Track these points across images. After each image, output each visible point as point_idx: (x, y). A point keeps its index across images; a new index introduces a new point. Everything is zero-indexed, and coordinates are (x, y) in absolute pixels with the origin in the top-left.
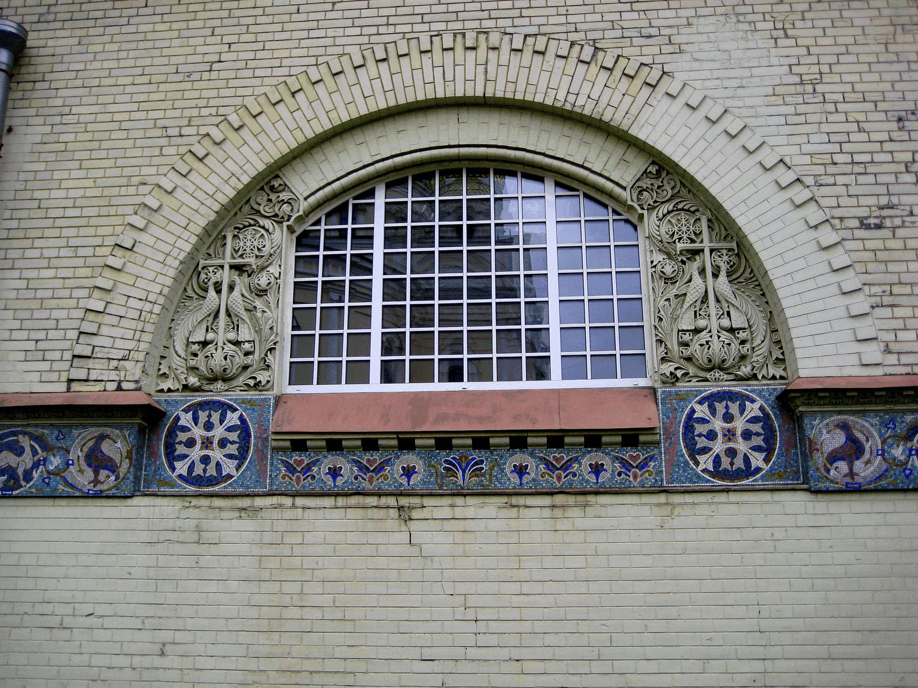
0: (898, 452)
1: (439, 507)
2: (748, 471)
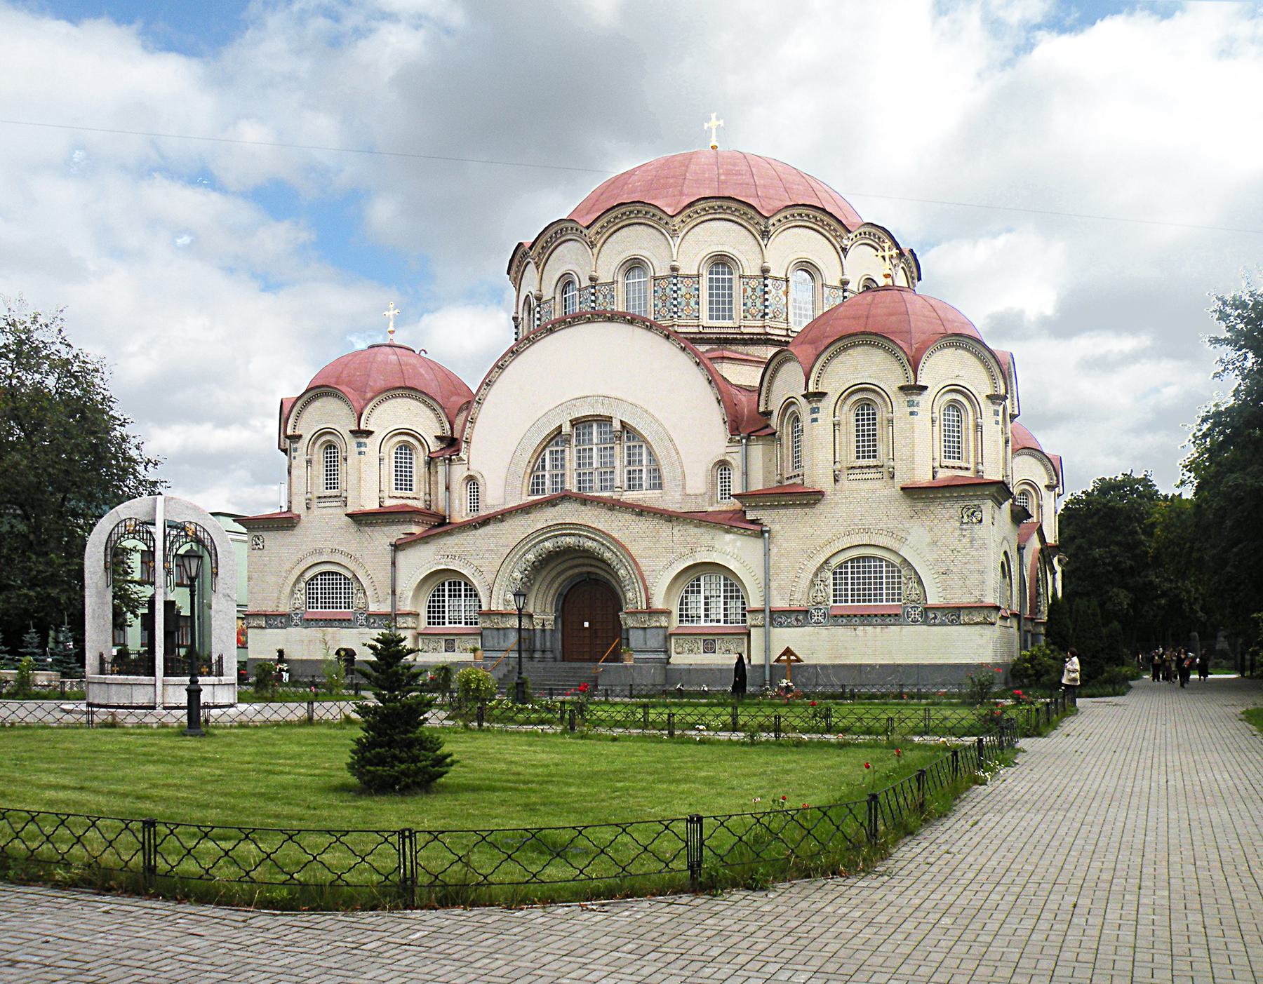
1: (861, 628)
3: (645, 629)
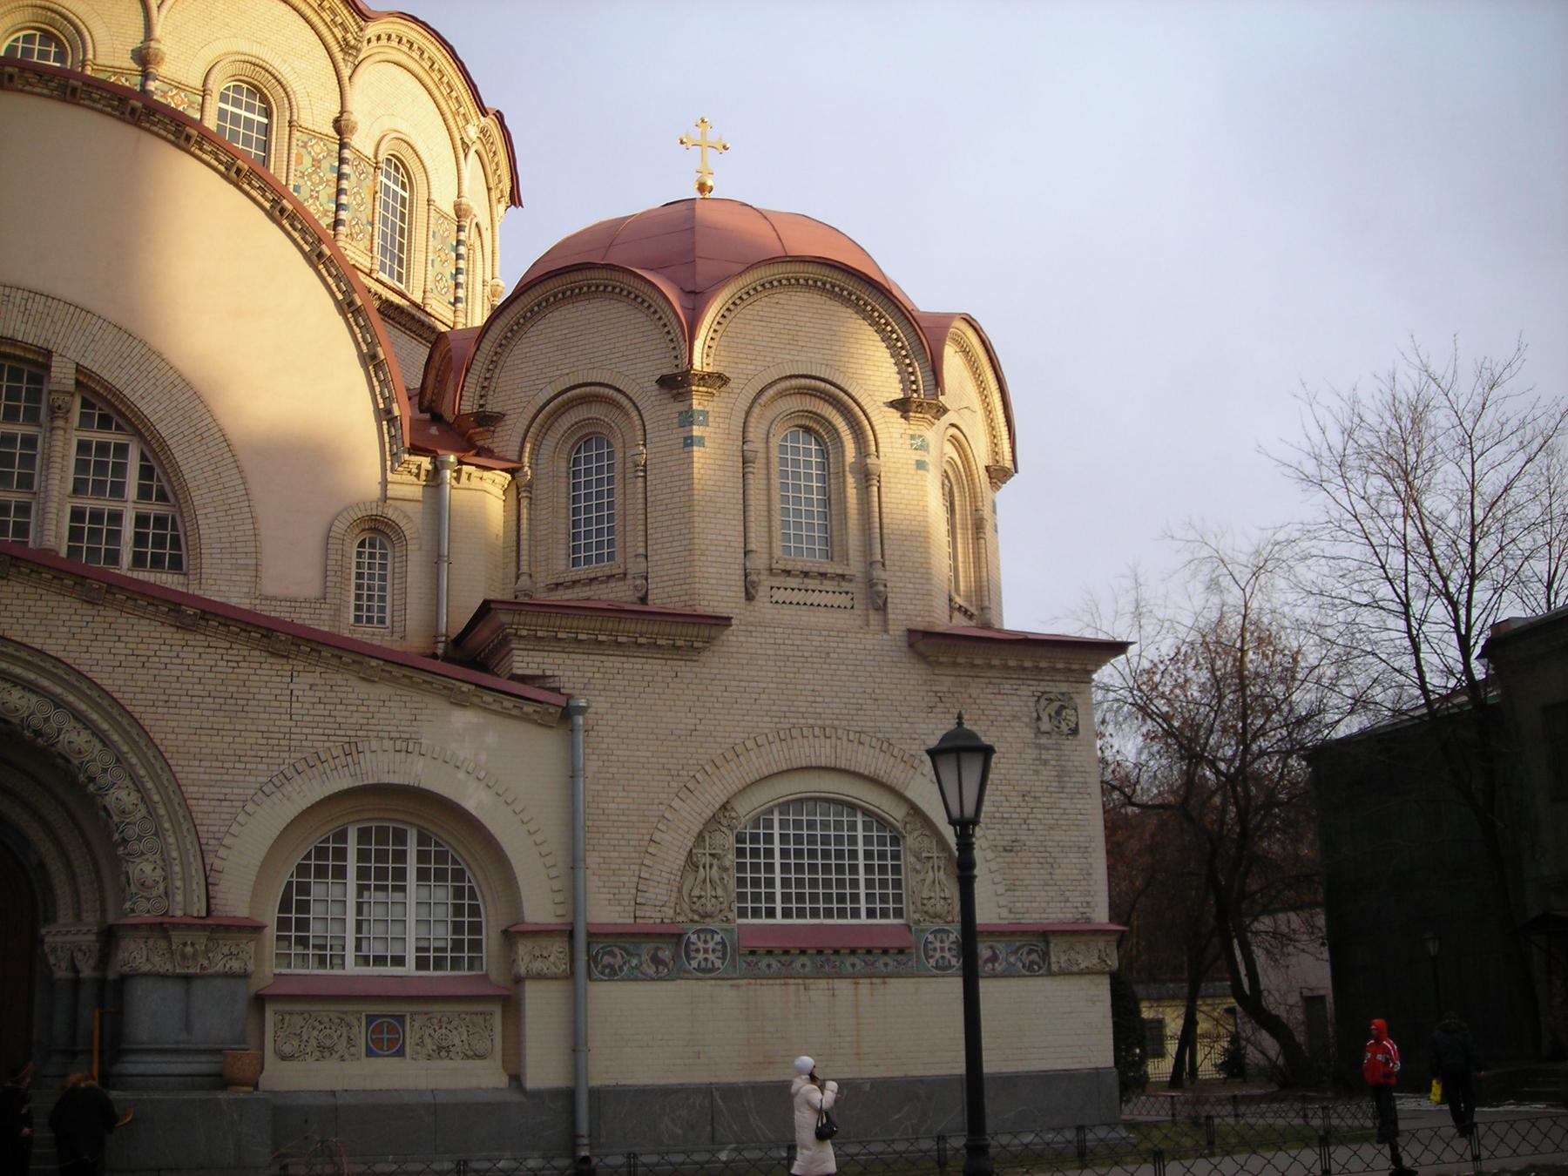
0: (1012, 959)
1: (822, 984)
2: (950, 967)
3: (188, 978)
